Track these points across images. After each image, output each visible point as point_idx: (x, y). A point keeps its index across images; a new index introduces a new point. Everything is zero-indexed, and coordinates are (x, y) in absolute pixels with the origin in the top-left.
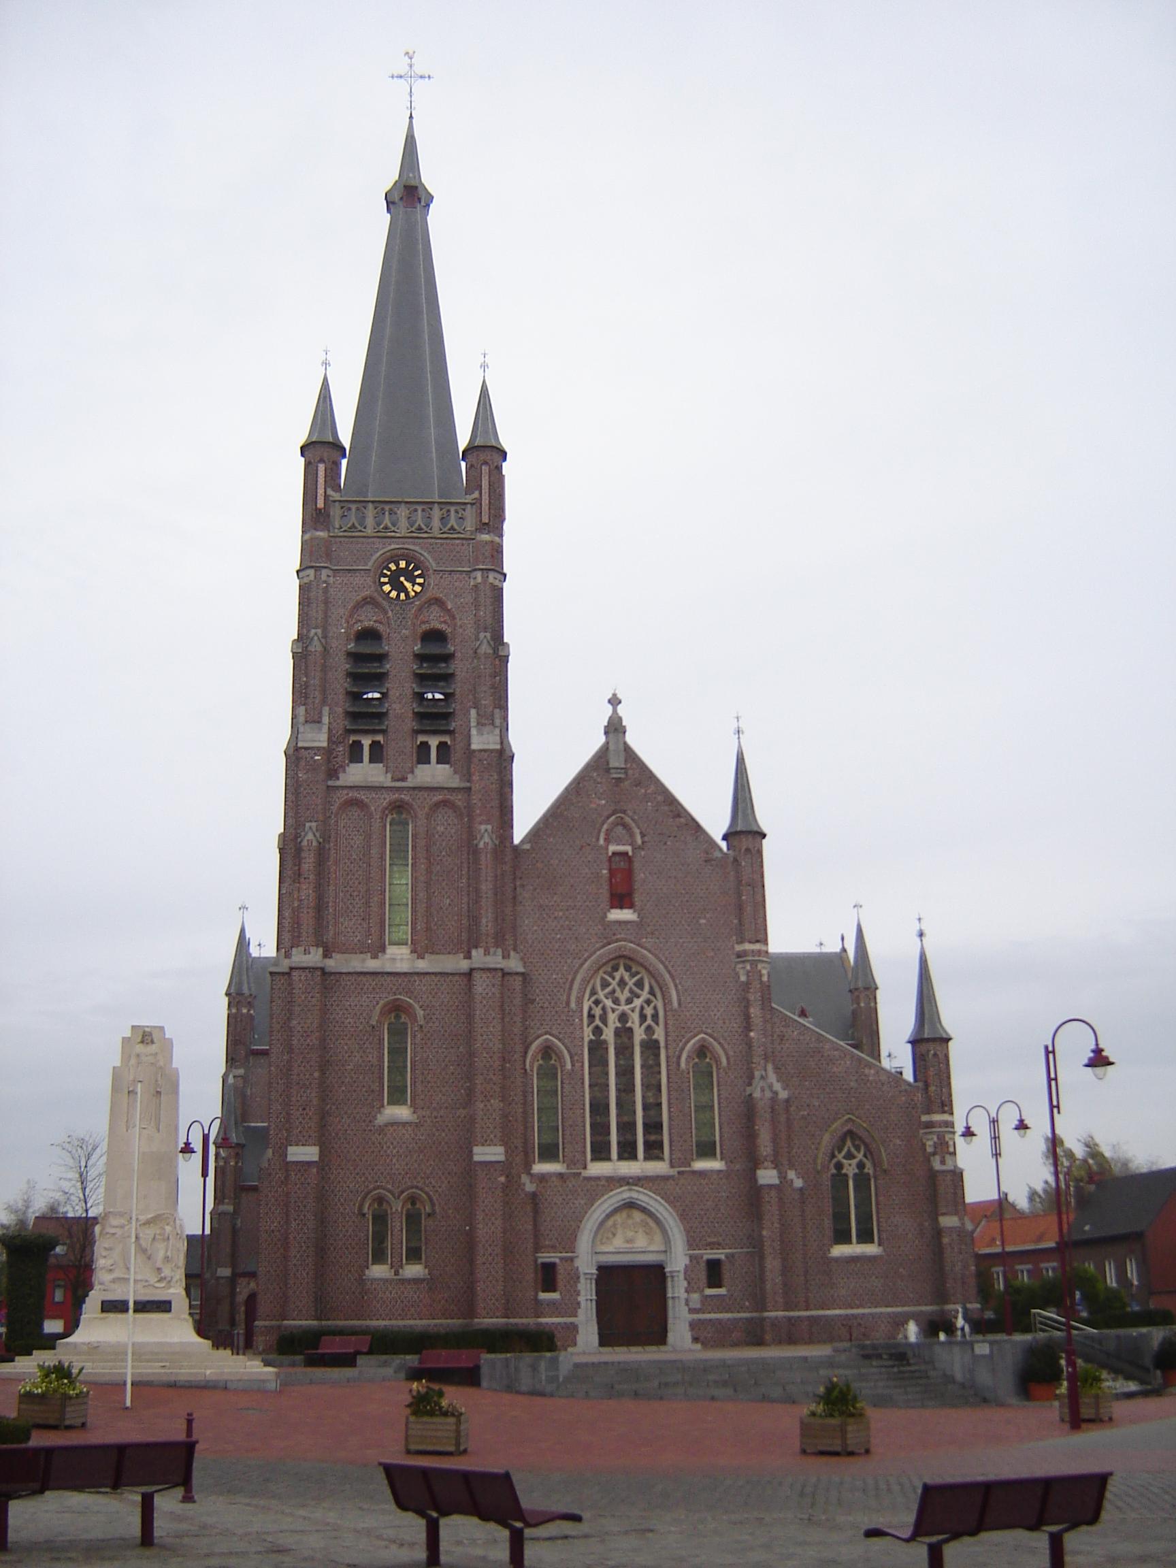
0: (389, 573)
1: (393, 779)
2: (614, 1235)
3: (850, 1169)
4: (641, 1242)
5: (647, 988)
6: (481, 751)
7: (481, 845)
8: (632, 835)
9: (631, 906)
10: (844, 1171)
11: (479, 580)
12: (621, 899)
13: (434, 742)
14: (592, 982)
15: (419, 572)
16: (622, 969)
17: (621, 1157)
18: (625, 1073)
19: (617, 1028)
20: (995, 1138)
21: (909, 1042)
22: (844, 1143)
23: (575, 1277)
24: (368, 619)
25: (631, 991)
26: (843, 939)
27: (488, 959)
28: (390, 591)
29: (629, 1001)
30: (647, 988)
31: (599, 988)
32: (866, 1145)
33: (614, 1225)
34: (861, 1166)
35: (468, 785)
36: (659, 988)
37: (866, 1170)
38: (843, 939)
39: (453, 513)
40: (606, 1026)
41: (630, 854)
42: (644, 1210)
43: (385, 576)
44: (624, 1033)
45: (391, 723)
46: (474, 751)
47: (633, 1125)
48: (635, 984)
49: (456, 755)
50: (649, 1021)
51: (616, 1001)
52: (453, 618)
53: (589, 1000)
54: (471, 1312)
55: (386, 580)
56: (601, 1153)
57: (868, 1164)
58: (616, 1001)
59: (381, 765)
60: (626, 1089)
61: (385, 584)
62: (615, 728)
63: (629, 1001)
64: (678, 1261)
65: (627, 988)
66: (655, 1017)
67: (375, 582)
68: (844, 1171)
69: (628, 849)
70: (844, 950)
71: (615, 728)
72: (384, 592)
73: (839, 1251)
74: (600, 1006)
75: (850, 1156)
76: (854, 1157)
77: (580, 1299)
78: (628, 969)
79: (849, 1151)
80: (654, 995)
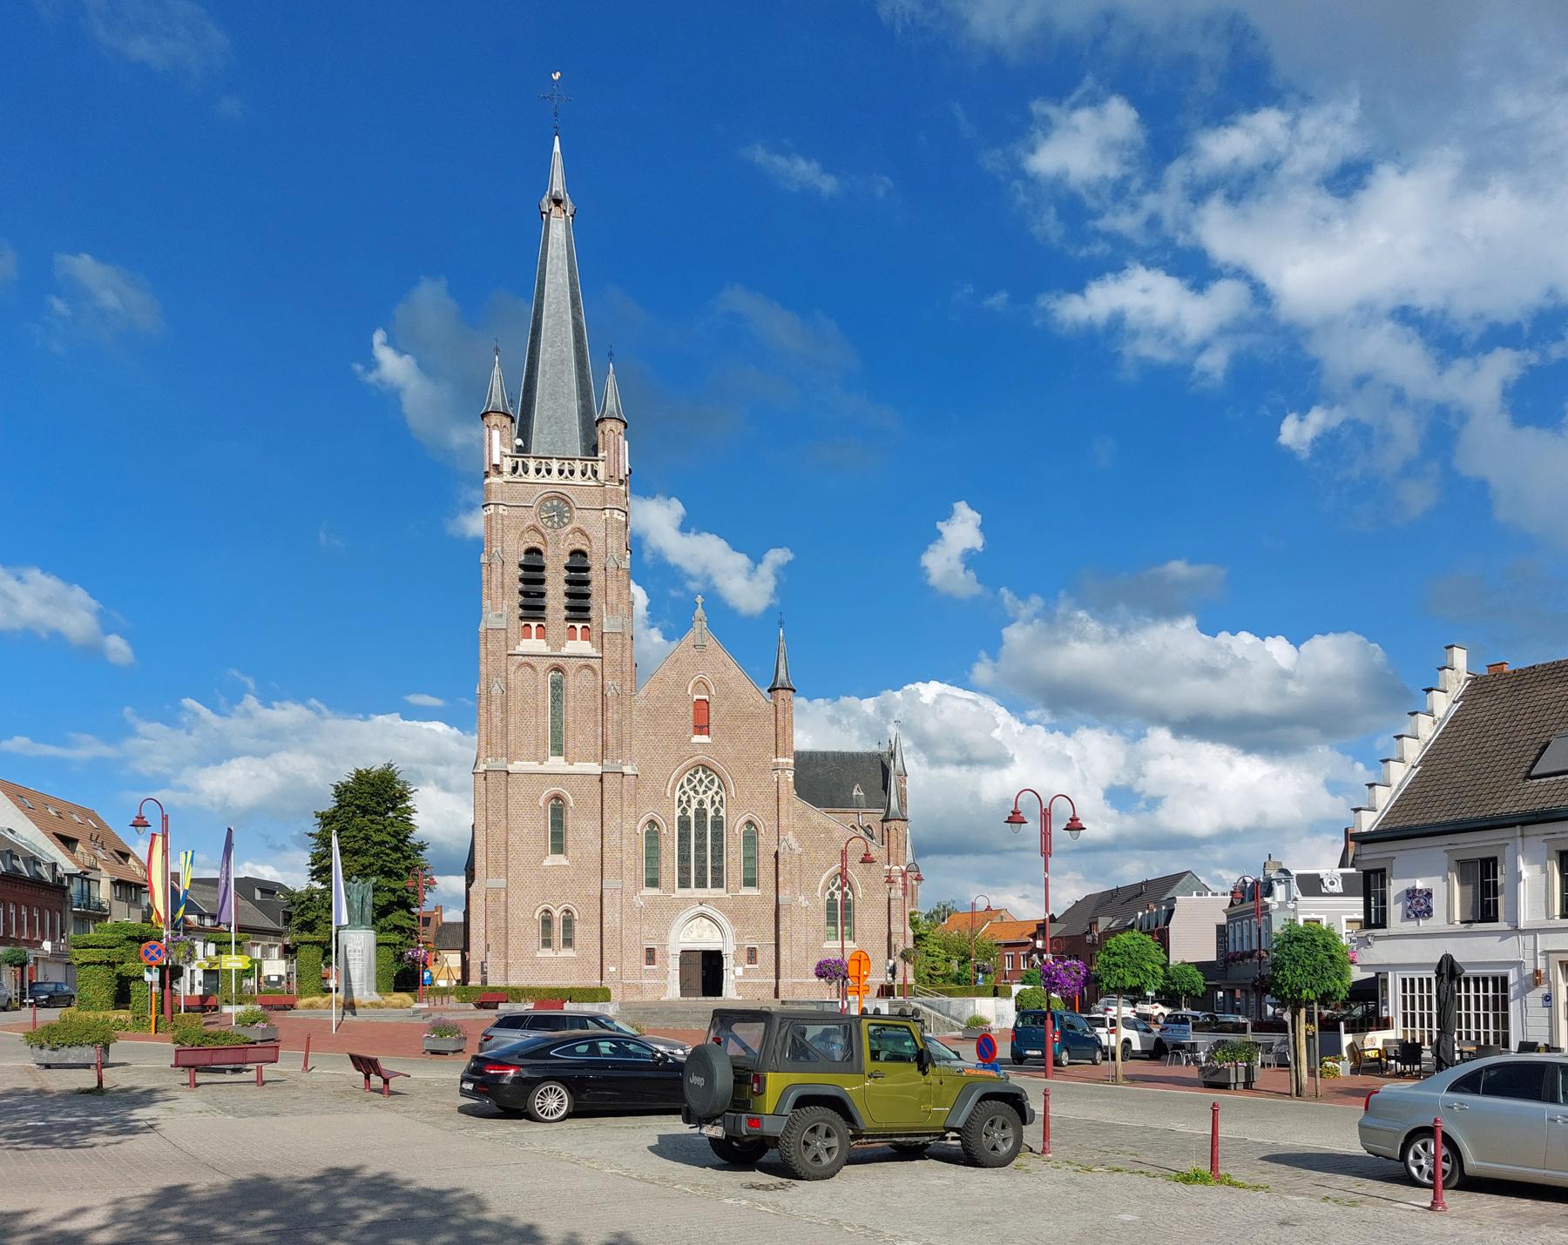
3: (838, 896)
4: (707, 935)
5: (716, 784)
11: (608, 515)
12: (702, 728)
16: (701, 771)
18: (701, 835)
19: (696, 809)
22: (836, 879)
23: (665, 955)
25: (706, 786)
29: (705, 792)
30: (716, 784)
31: (685, 784)
35: (601, 655)
36: (723, 785)
42: (709, 918)
44: (701, 813)
45: (548, 612)
47: (705, 868)
49: (595, 634)
50: (717, 804)
51: (696, 792)
52: (590, 541)
56: (684, 883)
57: (850, 894)
58: (696, 792)
59: (543, 641)
60: (701, 847)
63: (705, 792)
64: (729, 951)
65: (704, 784)
66: (721, 801)
69: (706, 697)
78: (704, 772)
80: (721, 789)
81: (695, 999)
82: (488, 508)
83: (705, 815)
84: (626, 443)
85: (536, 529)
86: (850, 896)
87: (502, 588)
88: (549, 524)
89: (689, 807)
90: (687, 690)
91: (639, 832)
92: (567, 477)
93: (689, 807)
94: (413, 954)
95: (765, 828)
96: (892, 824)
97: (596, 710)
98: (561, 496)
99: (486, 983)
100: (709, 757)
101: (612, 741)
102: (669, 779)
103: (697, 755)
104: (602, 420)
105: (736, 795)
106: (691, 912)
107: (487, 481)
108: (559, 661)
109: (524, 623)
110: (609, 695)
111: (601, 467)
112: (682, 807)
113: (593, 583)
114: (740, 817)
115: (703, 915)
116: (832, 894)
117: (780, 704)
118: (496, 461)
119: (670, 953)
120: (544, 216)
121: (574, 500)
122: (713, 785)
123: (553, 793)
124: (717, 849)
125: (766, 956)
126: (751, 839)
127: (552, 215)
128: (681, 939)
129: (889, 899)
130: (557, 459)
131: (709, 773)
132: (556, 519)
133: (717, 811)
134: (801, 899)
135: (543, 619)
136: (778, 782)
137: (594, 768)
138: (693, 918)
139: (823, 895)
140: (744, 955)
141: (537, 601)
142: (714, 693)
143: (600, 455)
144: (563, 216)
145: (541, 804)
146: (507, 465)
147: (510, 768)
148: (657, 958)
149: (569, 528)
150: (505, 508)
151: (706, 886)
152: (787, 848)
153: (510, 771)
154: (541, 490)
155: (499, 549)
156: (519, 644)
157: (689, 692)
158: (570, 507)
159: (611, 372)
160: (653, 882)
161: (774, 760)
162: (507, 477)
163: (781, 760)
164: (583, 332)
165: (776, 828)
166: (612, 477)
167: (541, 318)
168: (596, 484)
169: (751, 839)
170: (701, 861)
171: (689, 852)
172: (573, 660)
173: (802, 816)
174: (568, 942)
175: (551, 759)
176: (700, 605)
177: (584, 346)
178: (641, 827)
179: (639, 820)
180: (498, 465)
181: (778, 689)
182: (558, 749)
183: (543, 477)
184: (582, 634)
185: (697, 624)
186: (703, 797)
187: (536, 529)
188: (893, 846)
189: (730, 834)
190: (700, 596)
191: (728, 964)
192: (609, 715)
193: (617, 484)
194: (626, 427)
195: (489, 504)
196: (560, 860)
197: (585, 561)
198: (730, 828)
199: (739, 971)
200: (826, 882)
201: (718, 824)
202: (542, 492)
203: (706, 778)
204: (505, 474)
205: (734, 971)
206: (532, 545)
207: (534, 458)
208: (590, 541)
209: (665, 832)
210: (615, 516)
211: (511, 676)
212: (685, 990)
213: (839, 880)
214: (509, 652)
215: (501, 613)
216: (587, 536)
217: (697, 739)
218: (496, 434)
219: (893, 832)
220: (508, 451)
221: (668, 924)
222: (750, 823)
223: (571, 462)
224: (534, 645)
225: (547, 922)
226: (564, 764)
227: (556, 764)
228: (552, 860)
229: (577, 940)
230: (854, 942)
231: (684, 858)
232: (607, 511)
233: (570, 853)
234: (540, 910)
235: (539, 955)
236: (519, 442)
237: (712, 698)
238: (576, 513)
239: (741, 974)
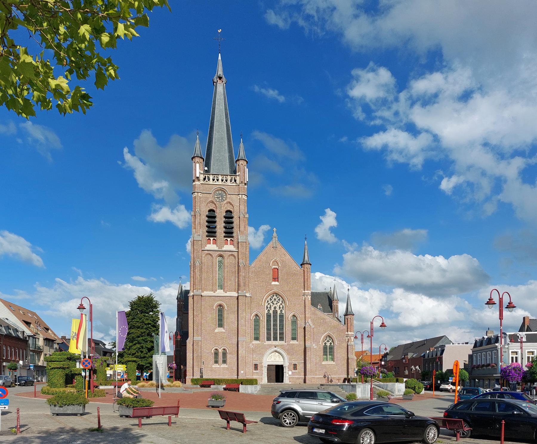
3: (328, 344)
4: (277, 359)
10: (327, 345)
11: (240, 197)
12: (275, 279)
16: (275, 296)
17: (274, 340)
18: (275, 320)
21: (344, 315)
22: (327, 338)
23: (262, 367)
24: (212, 207)
25: (277, 301)
26: (331, 288)
28: (217, 200)
29: (276, 304)
30: (281, 301)
32: (332, 339)
34: (331, 344)
35: (237, 251)
36: (284, 301)
37: (332, 345)
38: (331, 288)
42: (279, 353)
44: (275, 312)
45: (217, 234)
48: (278, 300)
50: (281, 309)
51: (273, 304)
52: (233, 207)
56: (269, 339)
57: (332, 343)
58: (273, 304)
59: (215, 245)
60: (275, 325)
63: (276, 304)
64: (286, 365)
65: (276, 301)
66: (283, 307)
68: (327, 345)
69: (277, 267)
70: (331, 291)
74: (270, 305)
75: (328, 341)
76: (329, 341)
78: (276, 296)
79: (328, 340)
80: (283, 303)
81: (273, 383)
83: (277, 312)
84: (247, 169)
85: (212, 202)
86: (332, 344)
87: (200, 224)
88: (218, 200)
89: (271, 309)
90: (270, 264)
91: (252, 319)
92: (225, 182)
93: (271, 309)
94: (171, 365)
95: (300, 318)
96: (349, 316)
97: (235, 272)
98: (222, 189)
99: (202, 377)
100: (278, 290)
101: (242, 284)
102: (263, 298)
103: (274, 289)
104: (238, 160)
106: (272, 350)
107: (194, 183)
108: (221, 253)
109: (208, 238)
110: (241, 266)
111: (238, 179)
113: (235, 223)
114: (290, 314)
115: (276, 351)
116: (325, 343)
117: (306, 270)
118: (198, 175)
119: (263, 366)
120: (215, 83)
121: (228, 191)
122: (280, 301)
123: (218, 304)
124: (281, 326)
125: (301, 367)
126: (294, 322)
127: (218, 83)
129: (348, 345)
130: (221, 175)
131: (278, 296)
132: (220, 198)
133: (281, 311)
134: (314, 345)
135: (215, 236)
136: (305, 300)
137: (235, 294)
139: (322, 343)
140: (292, 367)
141: (213, 230)
142: (280, 265)
143: (237, 174)
144: (222, 83)
145: (214, 308)
146: (202, 177)
147: (203, 294)
148: (259, 368)
149: (225, 202)
150: (201, 194)
151: (277, 340)
152: (309, 325)
153: (203, 295)
155: (199, 209)
156: (206, 246)
157: (271, 265)
158: (226, 194)
159: (241, 142)
160: (257, 339)
161: (303, 292)
162: (202, 182)
163: (306, 291)
164: (230, 128)
165: (304, 318)
166: (242, 182)
167: (214, 122)
168: (236, 185)
169: (294, 322)
170: (275, 330)
171: (271, 327)
173: (314, 314)
174: (224, 362)
175: (218, 291)
176: (275, 232)
177: (230, 133)
178: (253, 317)
179: (252, 314)
180: (199, 177)
181: (305, 264)
182: (221, 287)
184: (230, 243)
185: (274, 239)
186: (276, 306)
187: (212, 202)
188: (349, 325)
189: (287, 320)
190: (275, 228)
191: (286, 370)
192: (241, 273)
193: (244, 185)
194: (247, 163)
195: (195, 192)
196: (221, 330)
197: (232, 215)
199: (290, 373)
200: (324, 338)
201: (282, 316)
202: (215, 188)
203: (277, 298)
204: (201, 180)
206: (211, 208)
207: (212, 174)
208: (233, 207)
209: (262, 319)
210: (243, 197)
212: (269, 381)
214: (202, 249)
215: (199, 234)
216: (232, 205)
217: (273, 283)
218: (198, 165)
219: (349, 320)
221: (263, 355)
222: (294, 316)
224: (212, 246)
225: (216, 354)
227: (220, 292)
228: (218, 330)
229: (228, 361)
230: (334, 362)
231: (269, 329)
232: (240, 195)
233: (225, 327)
234: (214, 349)
235: (213, 366)
236: (206, 169)
238: (228, 196)
239: (291, 374)
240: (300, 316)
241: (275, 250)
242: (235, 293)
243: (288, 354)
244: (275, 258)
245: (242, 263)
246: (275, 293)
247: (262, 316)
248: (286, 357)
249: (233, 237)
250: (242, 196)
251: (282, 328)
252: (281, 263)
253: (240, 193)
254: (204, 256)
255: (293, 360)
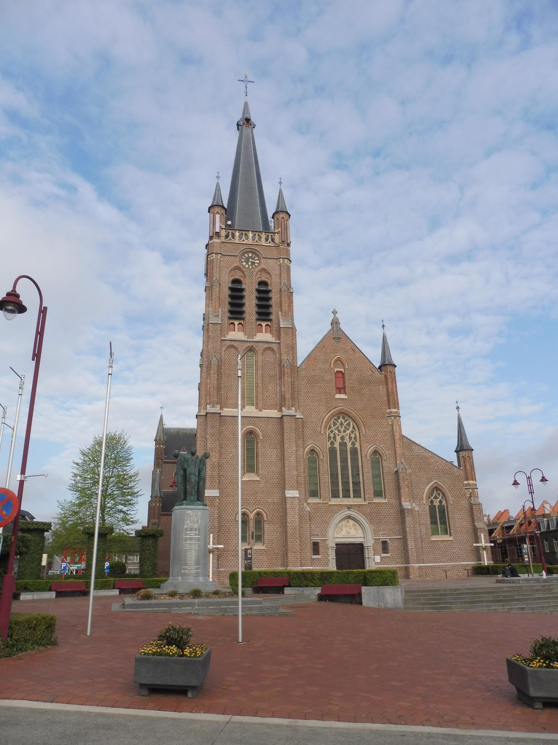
0: (245, 258)
1: (248, 338)
2: (342, 530)
3: (436, 503)
4: (353, 532)
6: (284, 328)
7: (285, 365)
8: (343, 365)
9: (345, 393)
12: (341, 390)
13: (264, 324)
14: (329, 424)
15: (257, 258)
16: (341, 418)
18: (344, 460)
19: (340, 442)
20: (530, 485)
25: (345, 427)
27: (290, 411)
28: (245, 265)
29: (344, 431)
30: (352, 426)
32: (443, 493)
33: (342, 526)
34: (441, 502)
35: (278, 341)
37: (443, 504)
39: (270, 237)
40: (336, 442)
41: (343, 372)
42: (354, 519)
43: (244, 259)
44: (343, 445)
45: (246, 315)
46: (281, 327)
49: (274, 328)
50: (353, 440)
51: (339, 431)
52: (271, 276)
53: (328, 431)
54: (285, 564)
55: (244, 260)
56: (335, 495)
58: (339, 431)
60: (344, 468)
61: (243, 262)
62: (335, 323)
63: (344, 431)
64: (369, 543)
65: (344, 426)
66: (355, 438)
67: (239, 261)
69: (342, 370)
71: (335, 323)
72: (243, 265)
73: (434, 538)
74: (333, 433)
75: (436, 498)
77: (329, 558)
78: (344, 418)
79: (435, 496)
82: (212, 255)
86: (444, 503)
90: (330, 365)
92: (257, 242)
102: (322, 422)
103: (339, 406)
105: (366, 433)
112: (331, 441)
113: (273, 300)
114: (369, 448)
115: (349, 517)
117: (389, 375)
128: (336, 536)
135: (243, 319)
137: (274, 413)
138: (343, 519)
140: (380, 547)
142: (347, 367)
146: (223, 233)
148: (321, 550)
150: (221, 256)
154: (242, 248)
155: (218, 278)
160: (314, 494)
161: (388, 411)
162: (223, 239)
166: (283, 242)
168: (275, 245)
172: (261, 344)
183: (244, 241)
189: (364, 459)
193: (286, 245)
198: (364, 456)
199: (378, 559)
201: (354, 451)
202: (243, 249)
205: (374, 559)
211: (223, 353)
213: (435, 492)
217: (338, 396)
220: (224, 227)
221: (327, 523)
222: (376, 452)
223: (260, 234)
224: (236, 334)
226: (256, 410)
230: (450, 536)
231: (334, 476)
232: (281, 260)
236: (229, 223)
237: (346, 371)
238: (263, 260)
239: (379, 561)
240: (387, 453)
241: (338, 342)
242: (275, 411)
243: (371, 521)
244: (338, 355)
245: (287, 361)
246: (343, 413)
247: (323, 453)
248: (368, 528)
249: (270, 320)
250: (284, 261)
251: (356, 475)
252: (348, 364)
253: (282, 257)
254: (224, 349)
255: (382, 534)
